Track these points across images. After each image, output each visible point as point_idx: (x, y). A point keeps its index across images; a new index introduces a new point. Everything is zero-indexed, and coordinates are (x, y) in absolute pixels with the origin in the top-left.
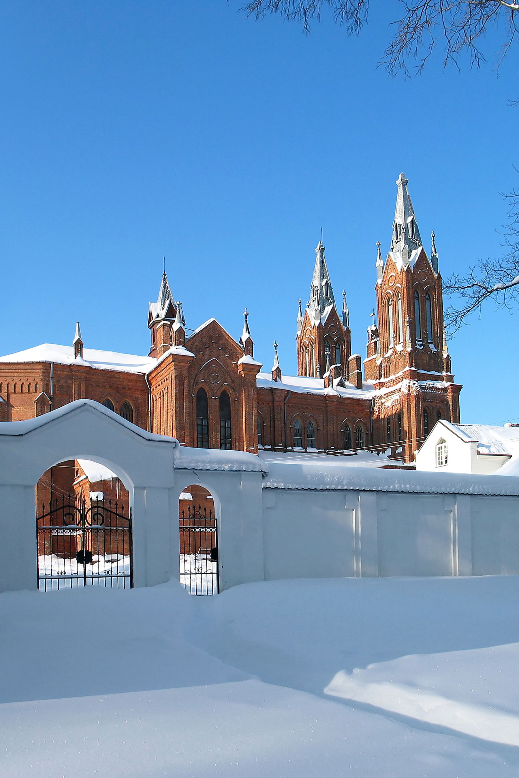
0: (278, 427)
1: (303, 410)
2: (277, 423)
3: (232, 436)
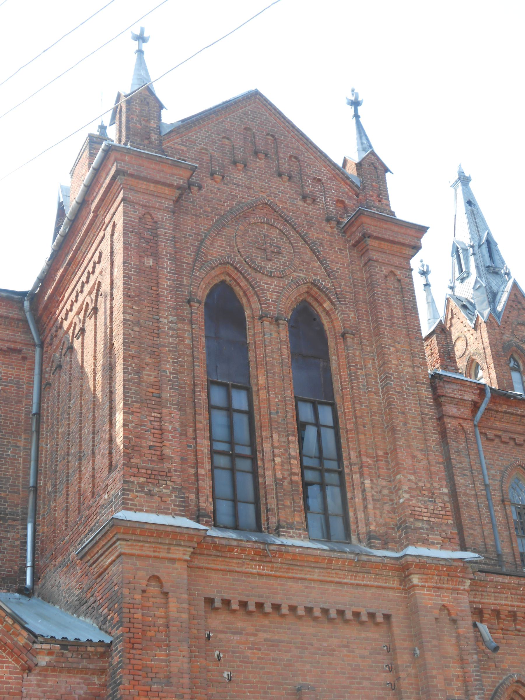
0: (466, 495)
2: (462, 481)
3: (344, 454)
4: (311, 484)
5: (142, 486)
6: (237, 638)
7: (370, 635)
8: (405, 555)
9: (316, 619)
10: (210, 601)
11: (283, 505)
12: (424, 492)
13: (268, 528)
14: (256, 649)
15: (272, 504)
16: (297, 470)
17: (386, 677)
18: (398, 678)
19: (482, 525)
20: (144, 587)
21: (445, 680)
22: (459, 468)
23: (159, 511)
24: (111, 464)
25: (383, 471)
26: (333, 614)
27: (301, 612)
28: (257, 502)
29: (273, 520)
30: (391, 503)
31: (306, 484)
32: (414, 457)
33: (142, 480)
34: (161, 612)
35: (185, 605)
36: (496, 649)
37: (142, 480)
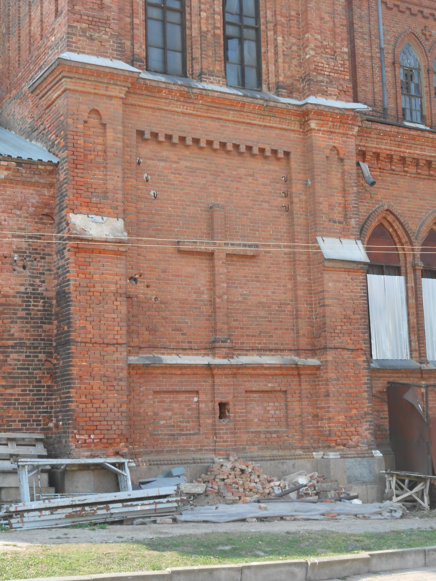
0: (363, 56)
1: (423, 20)
2: (361, 44)
3: (262, 13)
4: (231, 38)
5: (84, 31)
6: (162, 164)
7: (272, 167)
8: (307, 103)
9: (228, 152)
10: (141, 133)
11: (206, 55)
12: (327, 50)
13: (192, 74)
14: (178, 174)
15: (197, 53)
16: (219, 24)
17: (282, 201)
18: (292, 203)
19: (373, 83)
20: (86, 118)
21: (329, 205)
22: (360, 32)
23: (99, 54)
24: (57, 10)
25: (294, 30)
26: (243, 149)
27: (216, 146)
28: (183, 51)
29: (197, 67)
30: (298, 58)
31: (227, 38)
32: (322, 19)
33: (84, 25)
34: (100, 140)
35: (120, 135)
36: (373, 184)
37: (84, 25)
